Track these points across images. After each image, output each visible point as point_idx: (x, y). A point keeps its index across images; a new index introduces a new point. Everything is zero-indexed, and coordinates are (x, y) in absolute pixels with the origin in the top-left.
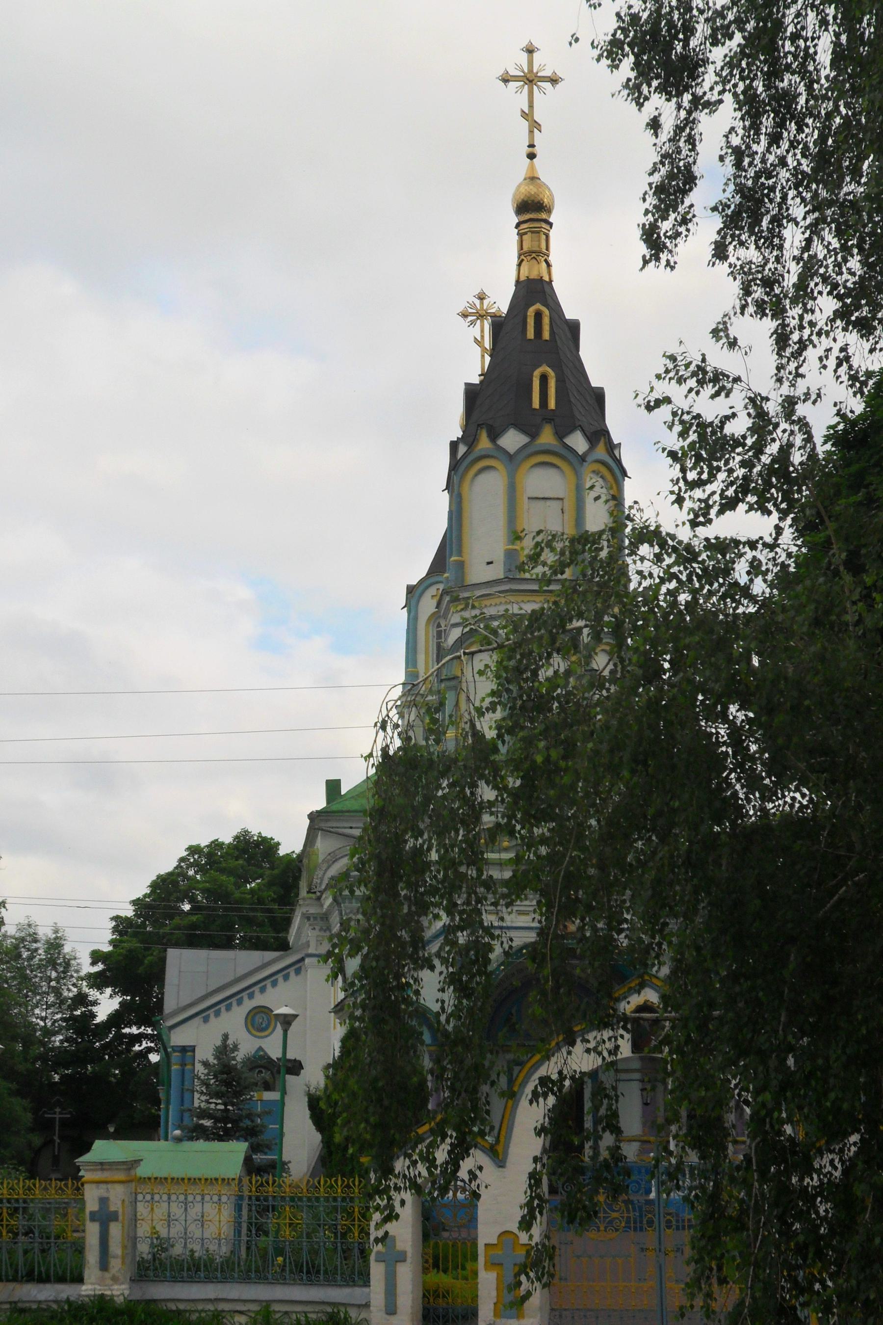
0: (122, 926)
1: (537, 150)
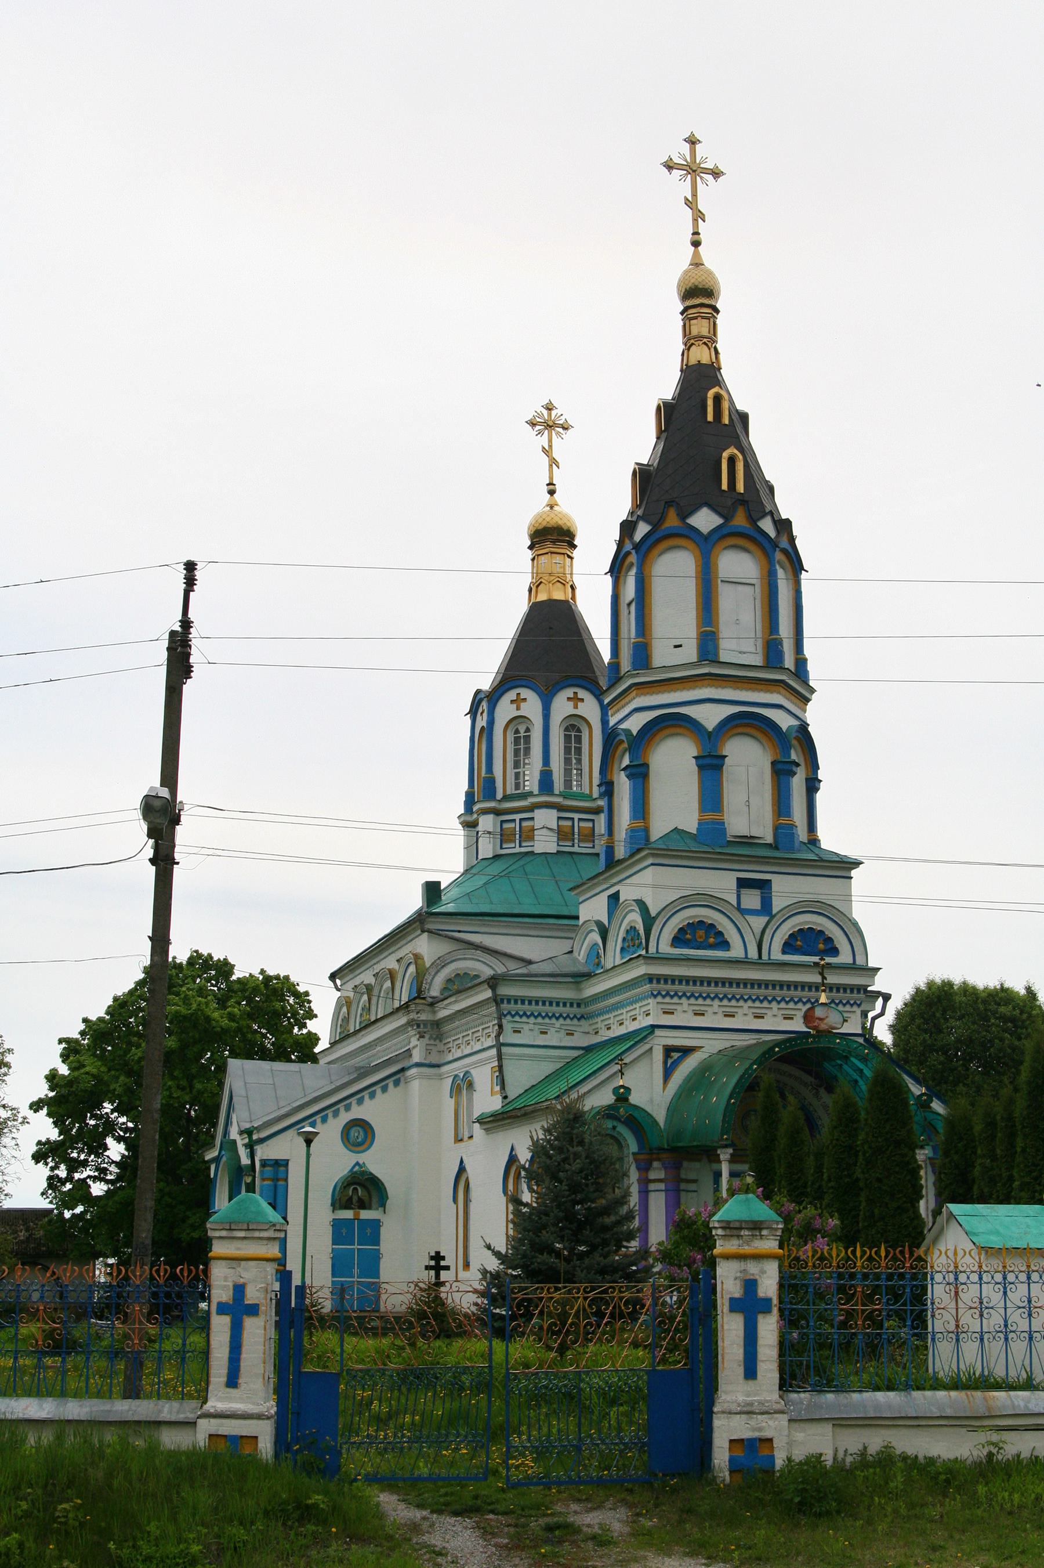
0: (71, 1050)
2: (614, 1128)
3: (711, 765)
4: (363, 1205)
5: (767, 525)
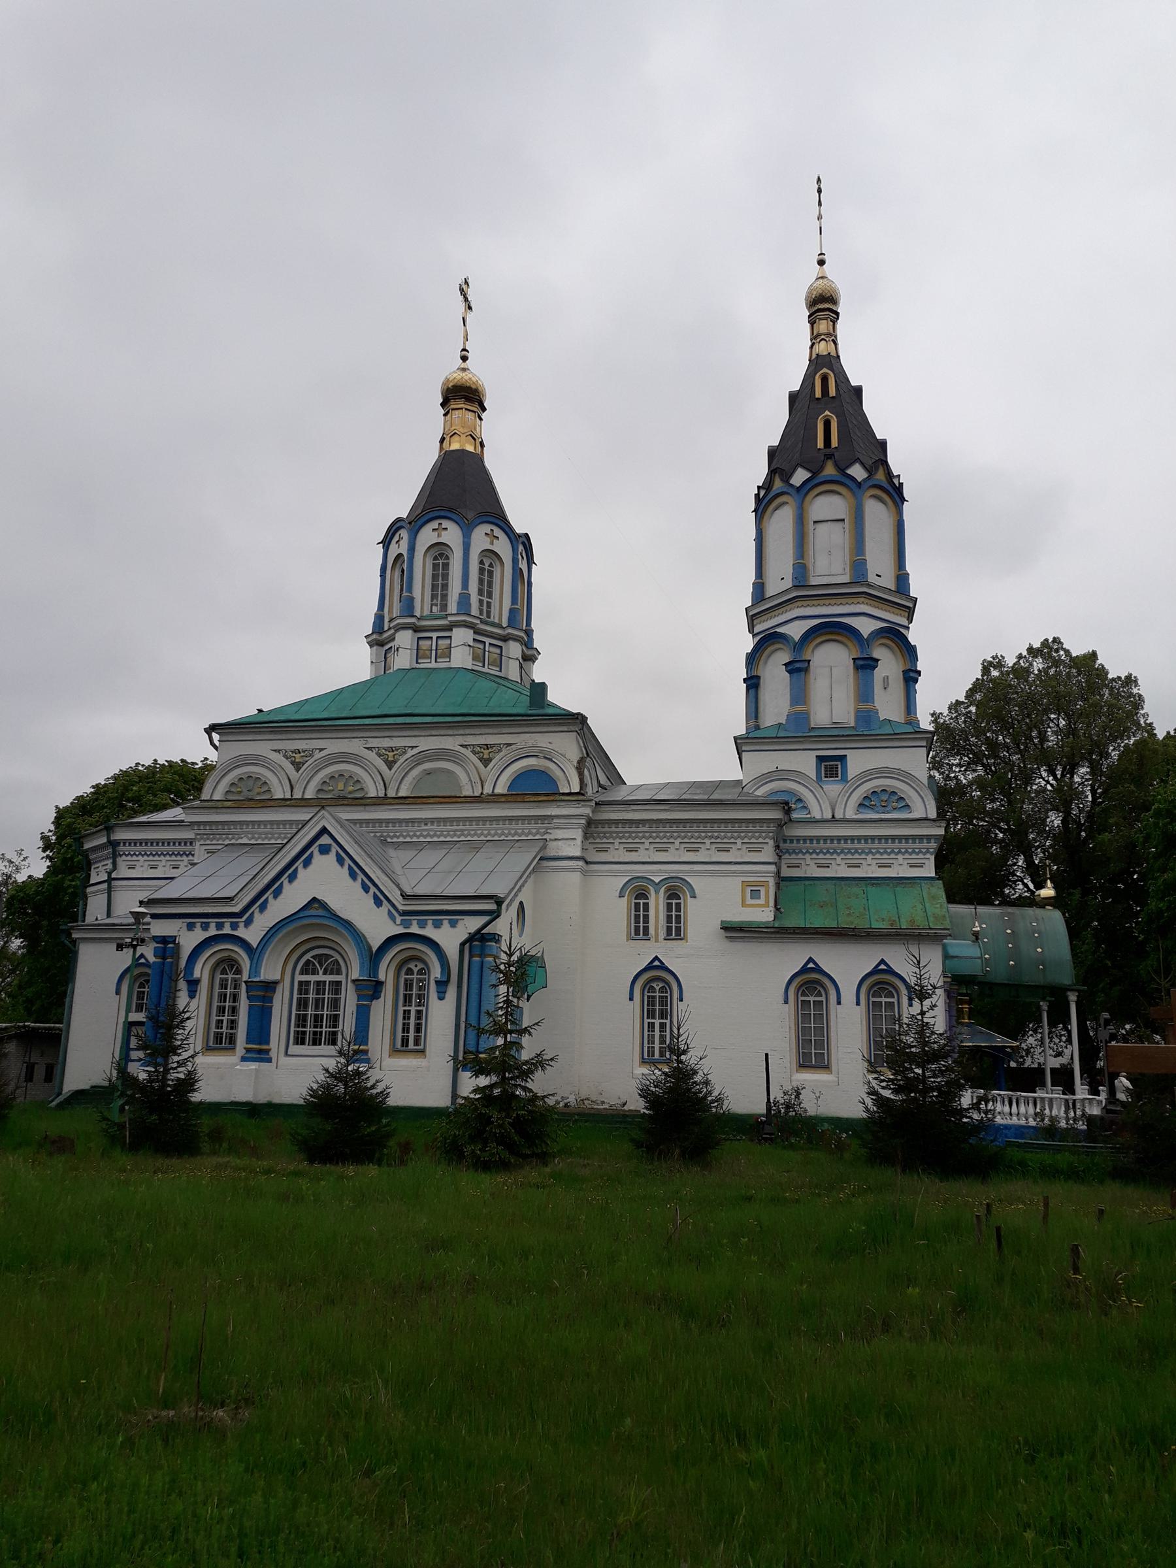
3: (798, 669)
5: (857, 472)
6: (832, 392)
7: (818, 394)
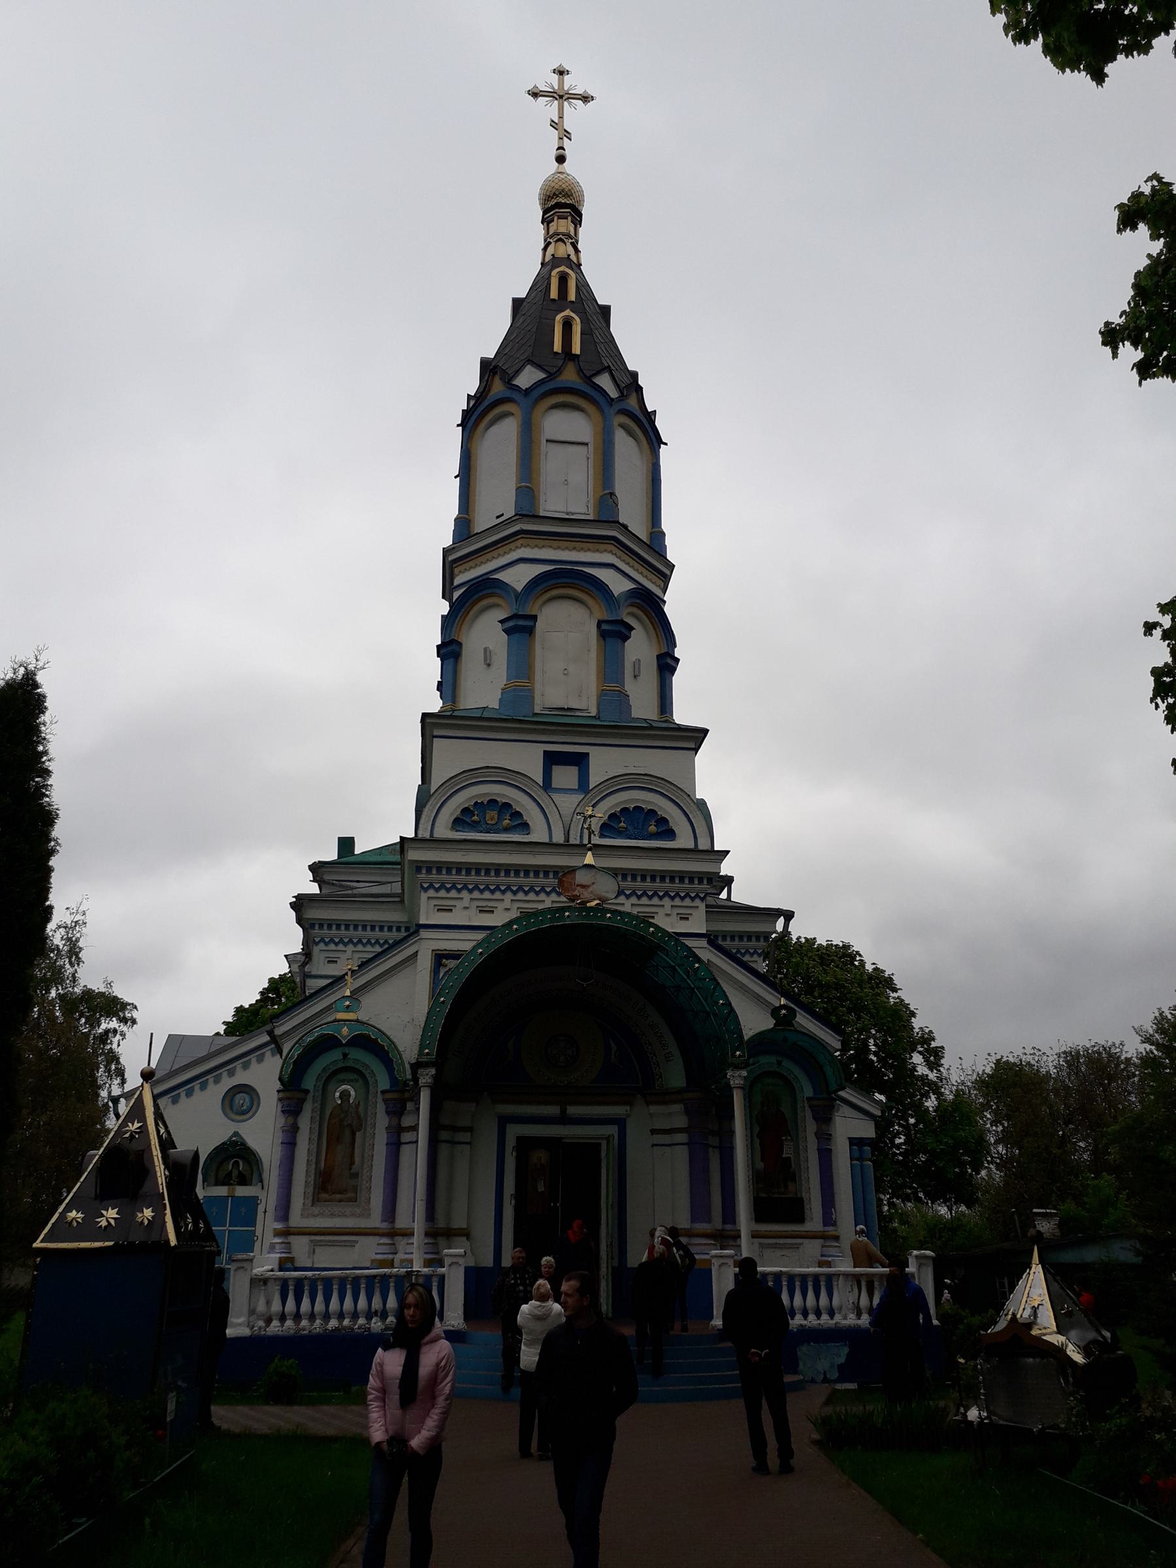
1: (567, 153)
2: (345, 1055)
3: (521, 628)
4: (244, 1181)
5: (604, 381)
6: (572, 296)
7: (554, 294)
